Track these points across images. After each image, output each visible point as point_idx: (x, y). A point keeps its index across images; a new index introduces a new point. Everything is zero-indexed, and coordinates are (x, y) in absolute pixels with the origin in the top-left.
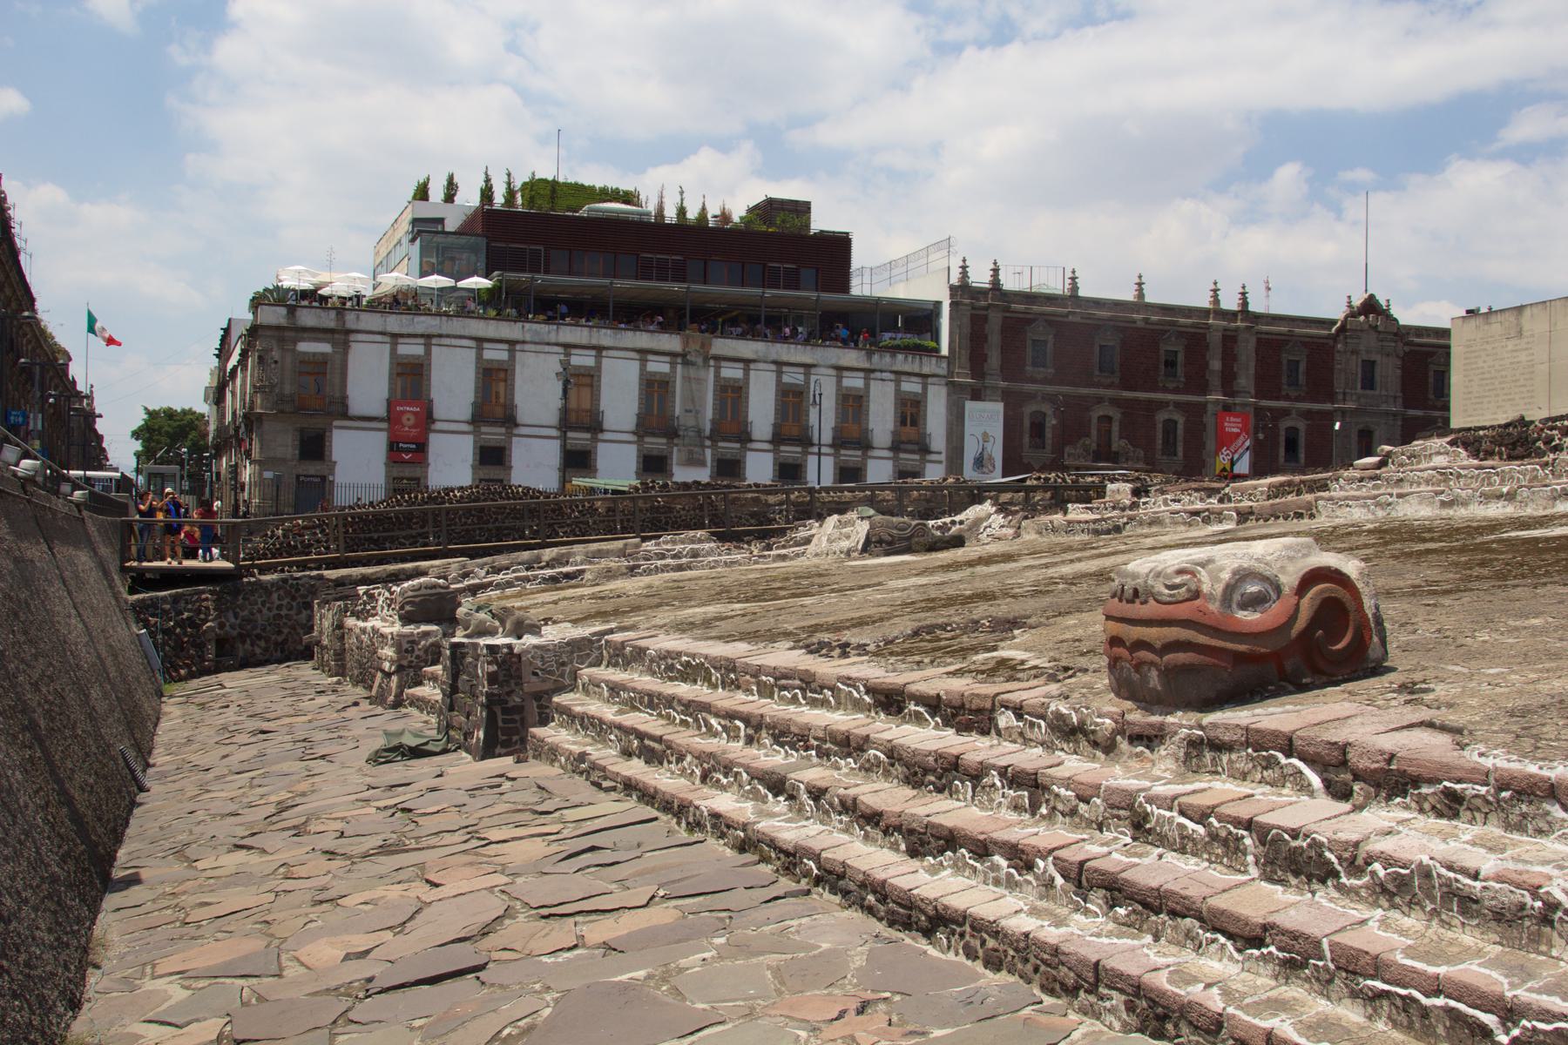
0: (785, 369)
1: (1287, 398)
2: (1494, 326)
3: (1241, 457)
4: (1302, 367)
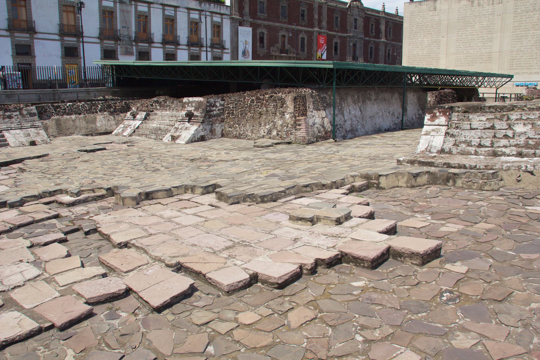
0: (166, 8)
1: (335, 31)
2: (423, 6)
3: (324, 53)
4: (339, 19)
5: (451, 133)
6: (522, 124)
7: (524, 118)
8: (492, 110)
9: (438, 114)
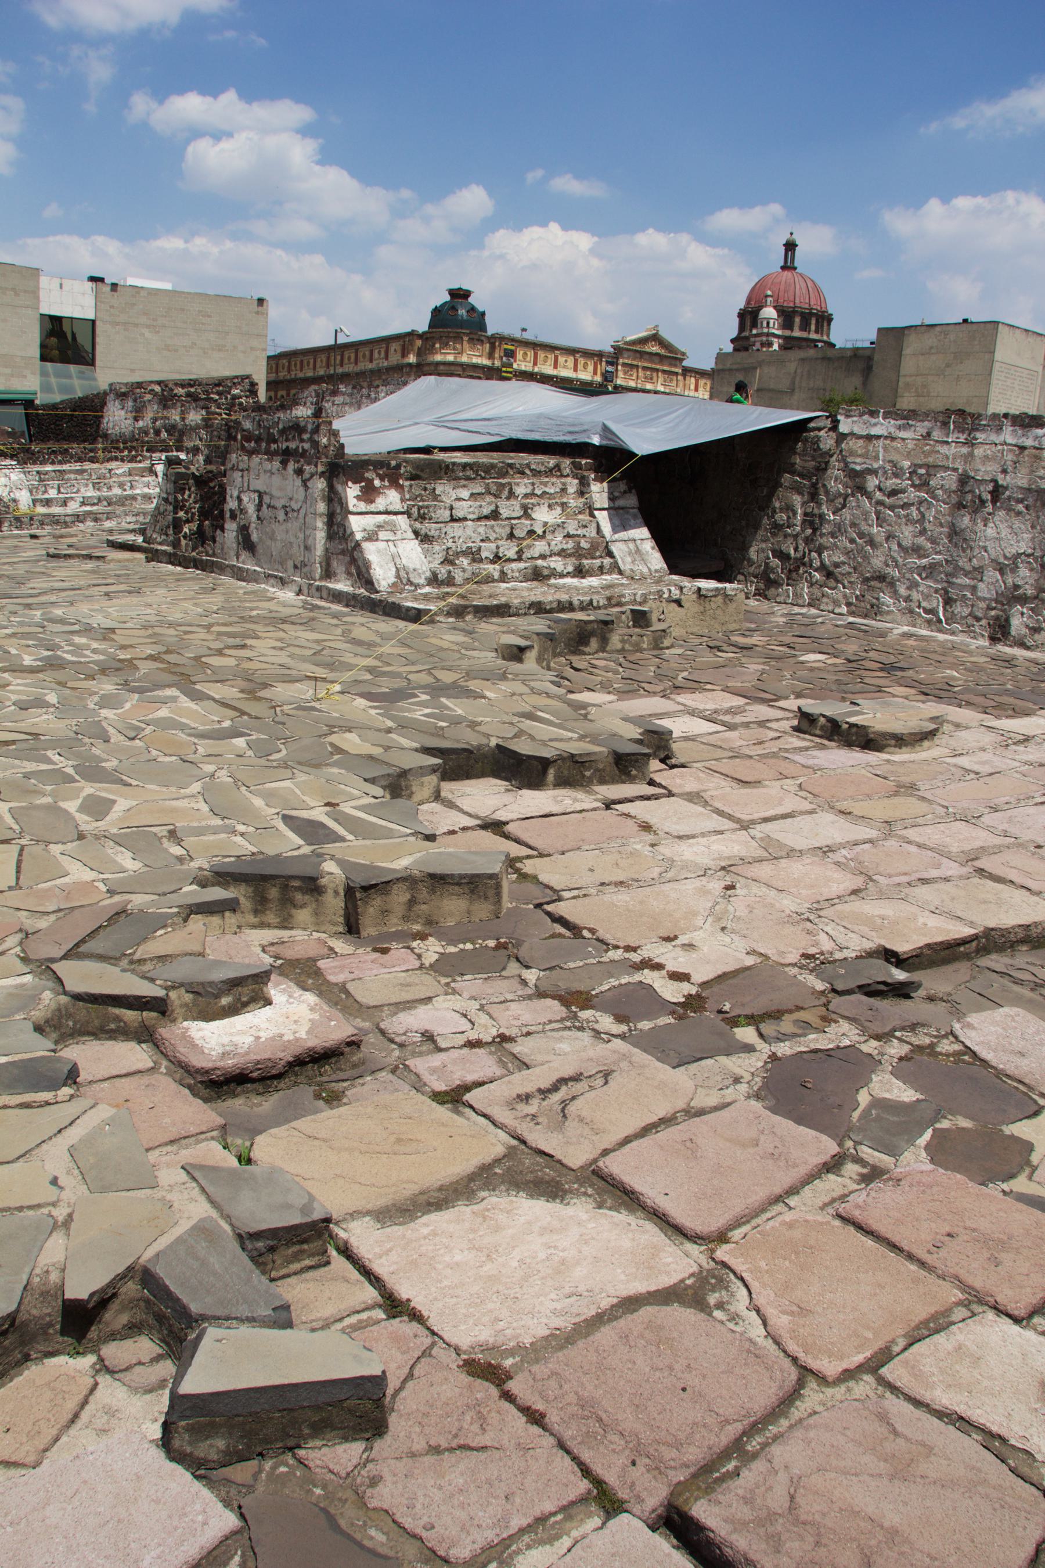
5: (423, 532)
6: (546, 505)
7: (538, 492)
8: (469, 473)
9: (377, 483)
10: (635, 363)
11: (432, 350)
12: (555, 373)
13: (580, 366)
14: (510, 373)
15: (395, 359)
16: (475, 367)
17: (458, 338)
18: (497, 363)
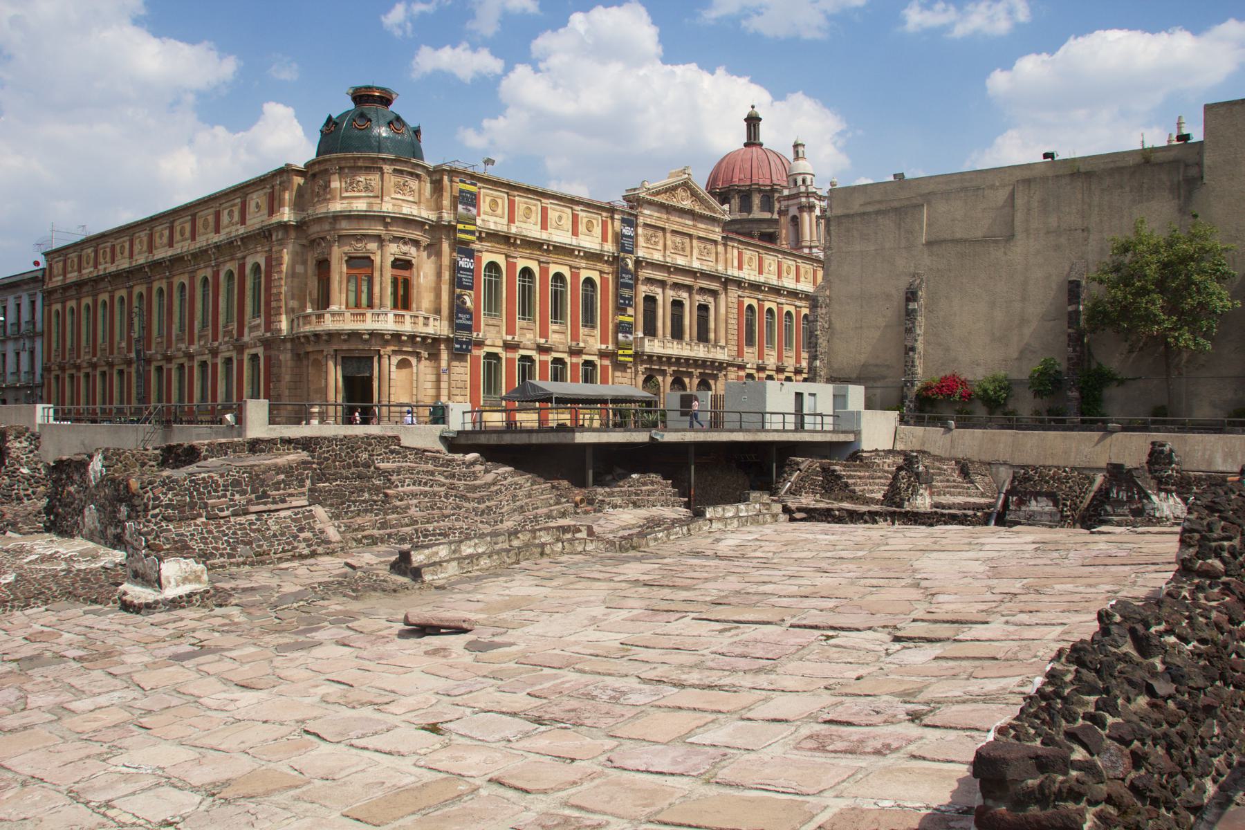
10: (660, 224)
11: (325, 193)
12: (544, 236)
13: (582, 228)
14: (472, 233)
15: (256, 220)
16: (408, 222)
17: (373, 167)
18: (447, 216)
